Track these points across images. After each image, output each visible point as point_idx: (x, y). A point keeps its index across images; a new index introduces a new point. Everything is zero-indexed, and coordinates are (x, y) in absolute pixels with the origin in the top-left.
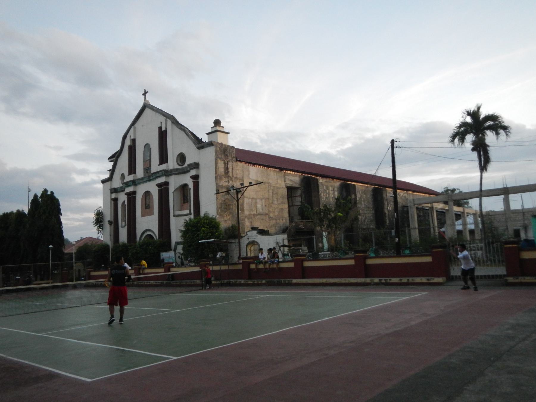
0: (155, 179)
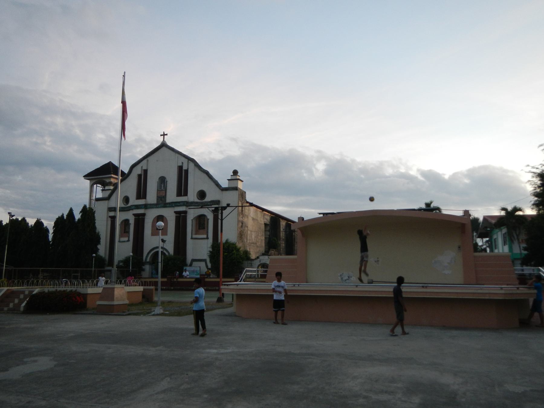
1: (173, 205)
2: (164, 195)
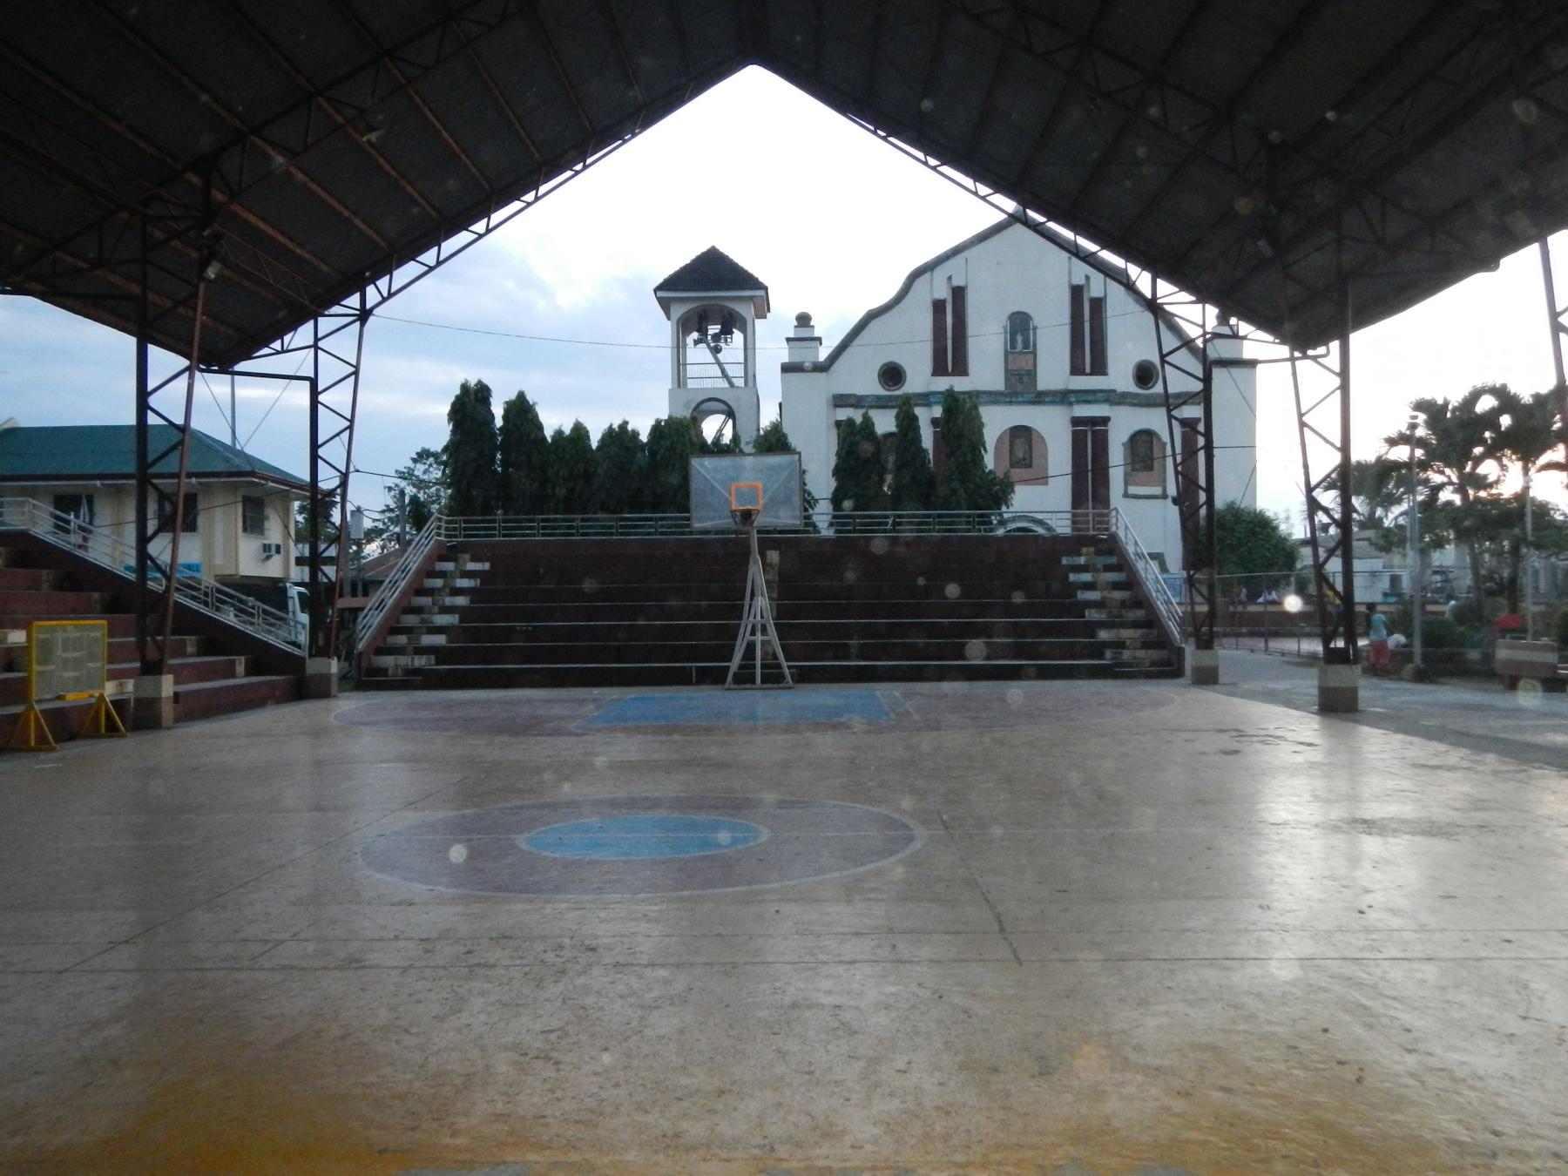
0: (1071, 404)
1: (1073, 399)
2: (1030, 367)
